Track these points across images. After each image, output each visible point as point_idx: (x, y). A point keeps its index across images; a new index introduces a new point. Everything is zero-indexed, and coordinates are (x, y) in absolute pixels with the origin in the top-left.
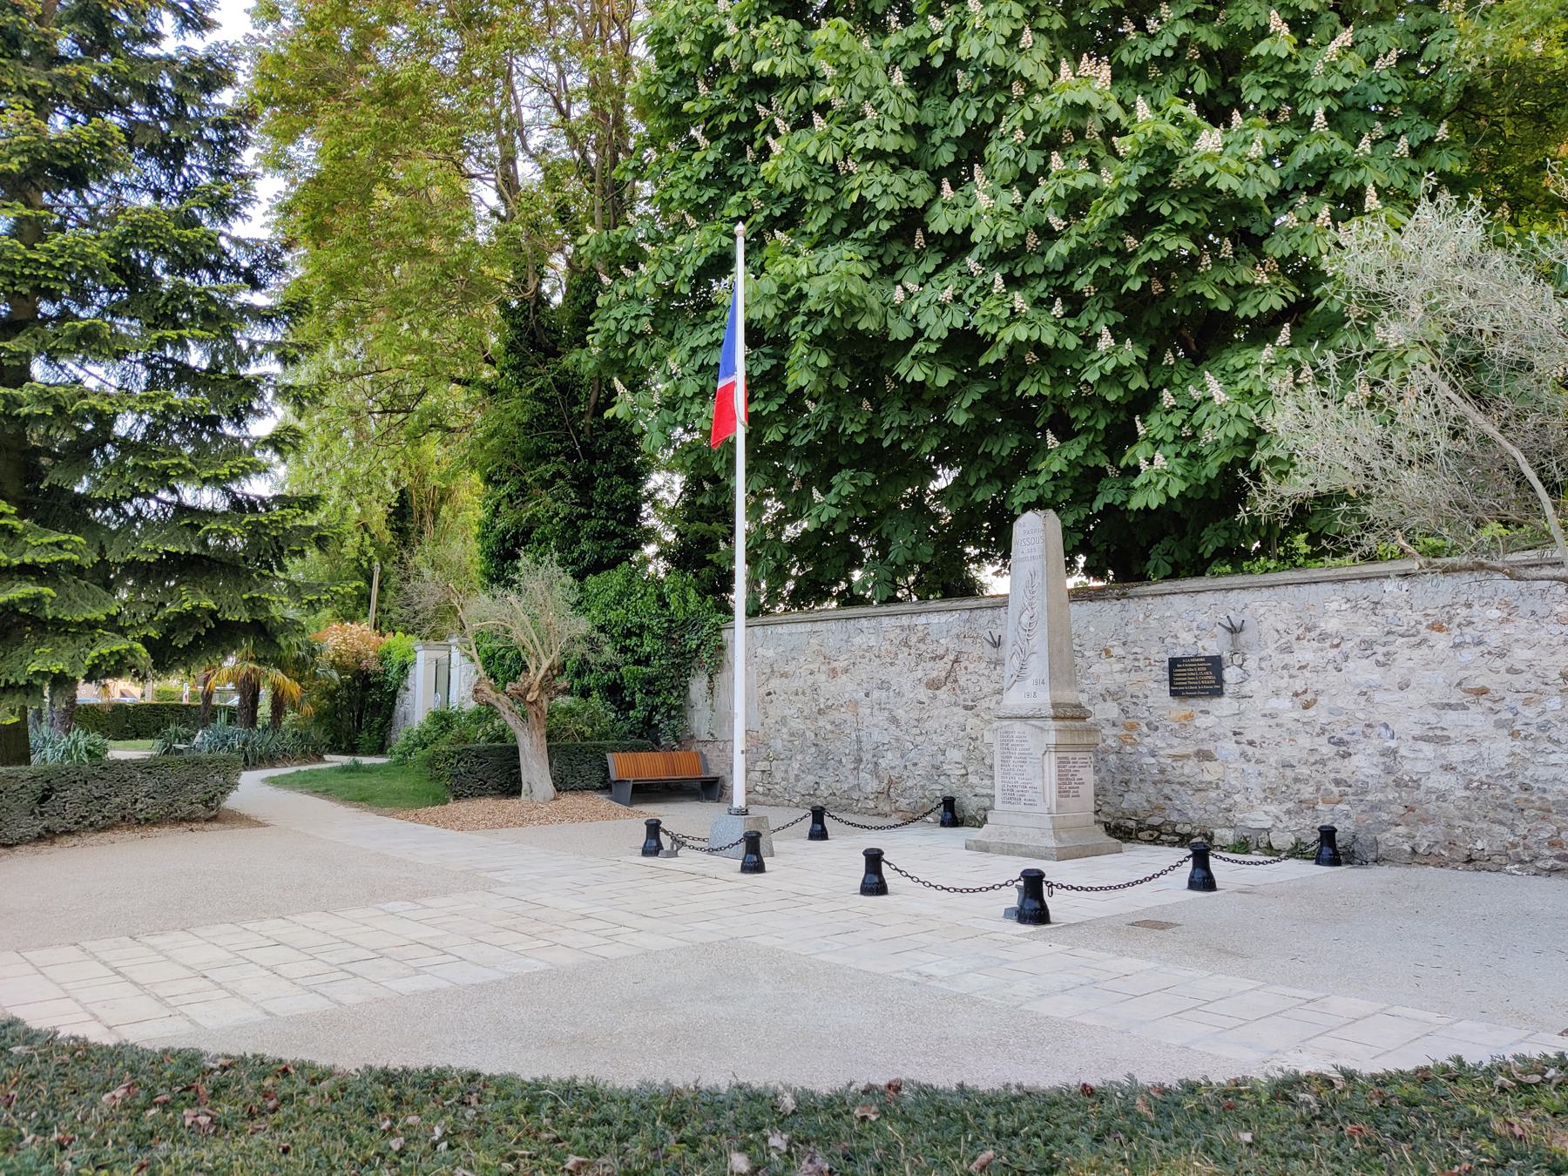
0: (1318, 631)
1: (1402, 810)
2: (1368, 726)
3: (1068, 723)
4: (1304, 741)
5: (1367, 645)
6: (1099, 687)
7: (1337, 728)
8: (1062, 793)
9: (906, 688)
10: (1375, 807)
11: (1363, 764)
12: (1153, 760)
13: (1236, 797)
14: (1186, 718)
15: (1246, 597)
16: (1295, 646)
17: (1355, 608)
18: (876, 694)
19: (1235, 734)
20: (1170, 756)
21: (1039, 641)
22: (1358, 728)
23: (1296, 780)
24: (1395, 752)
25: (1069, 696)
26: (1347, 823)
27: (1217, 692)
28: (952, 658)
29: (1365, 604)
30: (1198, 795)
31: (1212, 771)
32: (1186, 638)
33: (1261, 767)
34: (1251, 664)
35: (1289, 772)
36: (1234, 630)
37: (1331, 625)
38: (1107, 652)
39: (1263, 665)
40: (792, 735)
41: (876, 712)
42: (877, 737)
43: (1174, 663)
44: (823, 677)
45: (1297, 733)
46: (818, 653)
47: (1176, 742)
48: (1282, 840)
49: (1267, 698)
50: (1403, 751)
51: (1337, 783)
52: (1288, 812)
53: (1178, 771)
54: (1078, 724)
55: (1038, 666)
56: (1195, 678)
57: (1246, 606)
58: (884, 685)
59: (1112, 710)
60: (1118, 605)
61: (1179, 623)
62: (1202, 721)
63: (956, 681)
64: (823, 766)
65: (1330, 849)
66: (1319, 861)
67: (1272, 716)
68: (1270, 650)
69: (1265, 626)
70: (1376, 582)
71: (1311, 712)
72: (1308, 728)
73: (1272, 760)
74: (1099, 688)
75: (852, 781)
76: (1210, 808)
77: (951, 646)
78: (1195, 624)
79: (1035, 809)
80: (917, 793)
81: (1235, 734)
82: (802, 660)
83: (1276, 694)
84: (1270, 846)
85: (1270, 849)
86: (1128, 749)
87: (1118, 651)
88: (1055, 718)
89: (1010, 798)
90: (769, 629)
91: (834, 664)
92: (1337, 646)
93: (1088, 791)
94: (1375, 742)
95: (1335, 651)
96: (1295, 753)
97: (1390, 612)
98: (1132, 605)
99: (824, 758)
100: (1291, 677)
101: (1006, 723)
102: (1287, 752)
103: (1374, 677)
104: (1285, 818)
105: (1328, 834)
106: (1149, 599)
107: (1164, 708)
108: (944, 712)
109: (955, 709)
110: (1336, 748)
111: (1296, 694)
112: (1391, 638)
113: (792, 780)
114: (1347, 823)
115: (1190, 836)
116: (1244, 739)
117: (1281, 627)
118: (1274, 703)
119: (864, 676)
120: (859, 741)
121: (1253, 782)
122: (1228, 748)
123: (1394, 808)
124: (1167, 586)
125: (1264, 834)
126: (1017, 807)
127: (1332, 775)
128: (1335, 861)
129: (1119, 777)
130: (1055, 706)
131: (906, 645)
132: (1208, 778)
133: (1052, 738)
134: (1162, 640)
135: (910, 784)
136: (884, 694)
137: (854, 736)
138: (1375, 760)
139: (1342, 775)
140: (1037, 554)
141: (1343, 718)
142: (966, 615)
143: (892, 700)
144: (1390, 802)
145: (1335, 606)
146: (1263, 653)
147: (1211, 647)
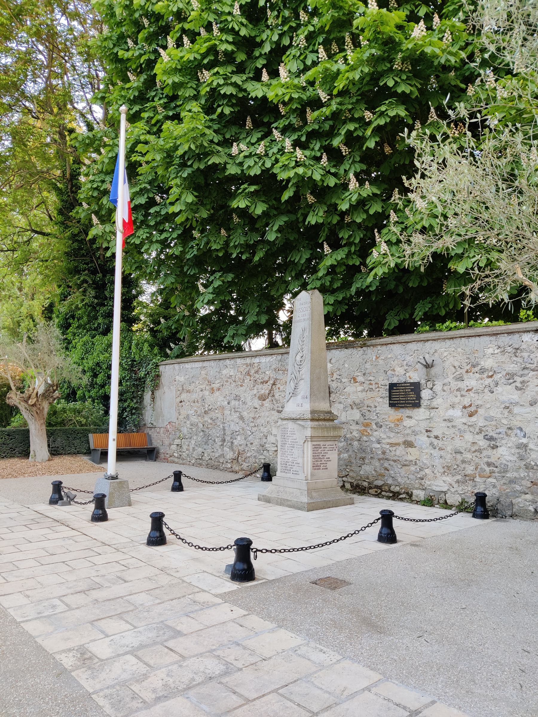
0: (479, 367)
1: (529, 484)
2: (510, 428)
3: (321, 423)
4: (469, 437)
5: (510, 376)
6: (349, 400)
7: (490, 430)
8: (315, 467)
9: (248, 400)
10: (512, 481)
11: (505, 453)
12: (378, 446)
13: (427, 471)
14: (398, 420)
15: (437, 345)
16: (465, 377)
17: (503, 352)
18: (233, 403)
19: (427, 431)
20: (388, 444)
21: (306, 372)
22: (503, 430)
23: (463, 462)
24: (526, 446)
25: (324, 406)
26: (494, 491)
27: (417, 405)
28: (272, 382)
29: (509, 349)
30: (404, 468)
31: (412, 454)
32: (400, 371)
33: (442, 453)
34: (438, 388)
35: (458, 456)
36: (428, 366)
37: (488, 363)
38: (355, 379)
39: (445, 388)
40: (192, 425)
41: (233, 413)
42: (234, 427)
43: (392, 386)
44: (207, 393)
45: (465, 431)
46: (205, 379)
47: (392, 435)
48: (454, 499)
49: (447, 409)
50: (531, 446)
51: (489, 464)
52: (458, 482)
53: (393, 453)
54: (327, 424)
55: (304, 388)
56: (405, 396)
57: (436, 351)
58: (237, 398)
59: (356, 415)
60: (361, 351)
61: (396, 362)
62: (407, 423)
63: (273, 396)
64: (206, 443)
65: (481, 508)
66: (475, 516)
67: (450, 421)
68: (450, 379)
69: (447, 364)
70: (517, 336)
71: (474, 419)
72: (471, 429)
73: (449, 449)
74: (350, 401)
75: (220, 452)
76: (411, 476)
77: (272, 375)
78: (405, 363)
79: (297, 477)
80: (252, 460)
81: (427, 431)
82: (197, 383)
83: (453, 406)
84: (446, 502)
85: (446, 505)
86: (365, 438)
87: (360, 379)
88: (312, 420)
89: (285, 471)
90: (182, 365)
91: (213, 385)
92: (491, 376)
93: (333, 466)
94: (513, 439)
95: (490, 380)
96: (463, 444)
97: (525, 355)
98: (369, 350)
99: (207, 439)
100: (462, 396)
101: (285, 422)
102: (458, 443)
103: (513, 397)
104: (455, 485)
105: (481, 498)
106: (379, 347)
107: (386, 414)
108: (267, 414)
109: (273, 412)
110: (488, 442)
111: (465, 407)
112: (526, 372)
113: (191, 450)
114: (494, 491)
115: (399, 493)
116: (432, 435)
117: (457, 364)
118: (451, 413)
119: (227, 393)
120: (224, 430)
121: (437, 462)
122: (422, 440)
123: (524, 482)
124: (390, 339)
125: (442, 495)
126: (288, 475)
127: (486, 460)
128: (485, 515)
129: (359, 455)
130: (313, 412)
131: (248, 374)
132: (410, 458)
133: (309, 433)
134: (386, 372)
135: (248, 455)
136: (237, 403)
137: (221, 426)
138: (513, 451)
139: (492, 460)
140: (307, 317)
141: (494, 423)
142: (279, 357)
143: (241, 406)
144: (522, 479)
145: (490, 351)
146: (446, 381)
147: (414, 377)
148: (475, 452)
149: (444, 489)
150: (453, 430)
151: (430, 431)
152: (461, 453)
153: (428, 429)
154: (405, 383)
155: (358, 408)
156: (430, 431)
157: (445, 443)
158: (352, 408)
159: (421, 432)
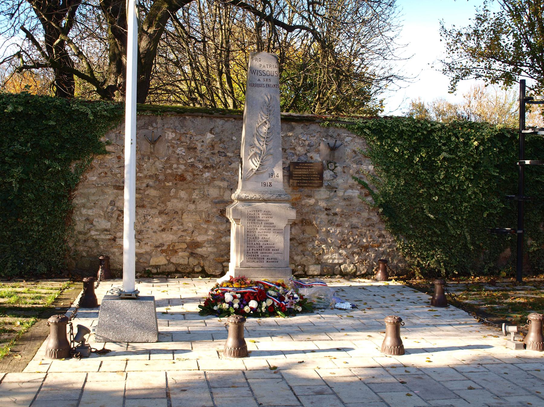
14: (296, 199)
32: (300, 150)
34: (339, 169)
78: (307, 143)
81: (326, 209)
118: (350, 192)
148: (369, 226)
151: (329, 209)
154: (306, 162)
156: (329, 209)
159: (320, 210)
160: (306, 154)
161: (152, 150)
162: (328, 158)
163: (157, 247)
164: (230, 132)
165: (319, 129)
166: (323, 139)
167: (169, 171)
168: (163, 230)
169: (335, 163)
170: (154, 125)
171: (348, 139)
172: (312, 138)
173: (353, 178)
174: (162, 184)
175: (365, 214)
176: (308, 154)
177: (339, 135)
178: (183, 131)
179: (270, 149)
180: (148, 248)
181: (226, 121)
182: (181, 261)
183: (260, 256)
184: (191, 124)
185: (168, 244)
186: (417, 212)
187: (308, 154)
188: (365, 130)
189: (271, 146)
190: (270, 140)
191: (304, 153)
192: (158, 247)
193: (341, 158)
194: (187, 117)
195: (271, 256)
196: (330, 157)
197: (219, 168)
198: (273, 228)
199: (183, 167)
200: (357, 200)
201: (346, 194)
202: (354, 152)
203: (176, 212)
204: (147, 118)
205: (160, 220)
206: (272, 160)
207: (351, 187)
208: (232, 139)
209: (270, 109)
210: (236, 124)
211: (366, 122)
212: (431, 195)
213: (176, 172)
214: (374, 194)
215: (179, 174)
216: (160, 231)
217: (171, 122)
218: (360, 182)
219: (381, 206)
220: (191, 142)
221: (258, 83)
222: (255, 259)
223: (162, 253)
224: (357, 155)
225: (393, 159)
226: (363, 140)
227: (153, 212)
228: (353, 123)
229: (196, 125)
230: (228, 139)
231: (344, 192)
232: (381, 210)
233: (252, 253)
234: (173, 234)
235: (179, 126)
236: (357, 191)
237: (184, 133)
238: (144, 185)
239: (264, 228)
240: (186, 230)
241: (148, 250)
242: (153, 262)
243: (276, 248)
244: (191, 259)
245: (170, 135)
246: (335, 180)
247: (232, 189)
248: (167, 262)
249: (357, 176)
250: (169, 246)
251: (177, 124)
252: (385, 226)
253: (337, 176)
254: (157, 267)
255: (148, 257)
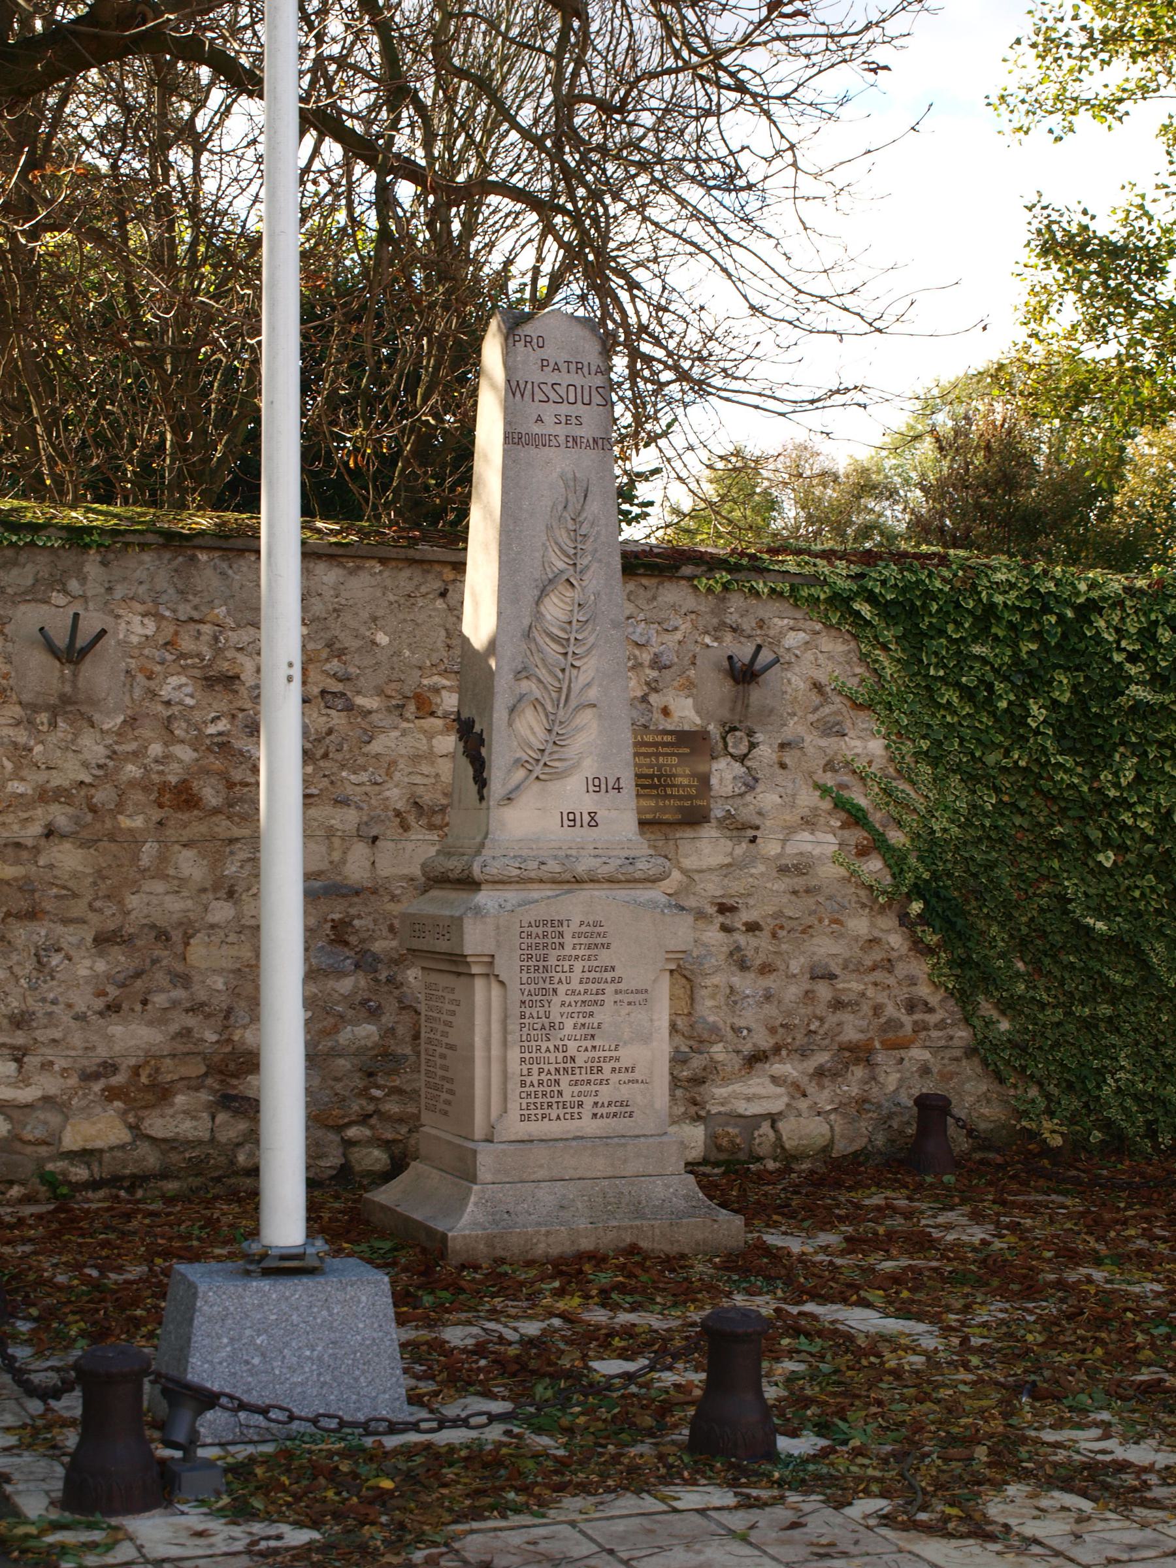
33: (769, 982)
34: (766, 752)
35: (824, 991)
49: (790, 830)
52: (819, 1073)
73: (795, 968)
81: (723, 909)
104: (811, 1089)
118: (805, 842)
125: (766, 1127)
148: (873, 969)
149: (776, 1106)
150: (810, 901)
152: (832, 977)
153: (730, 902)
155: (431, 827)
157: (784, 947)
158: (405, 827)
160: (644, 699)
161: (68, 689)
162: (725, 713)
163: (88, 1077)
164: (365, 615)
165: (690, 602)
166: (708, 640)
167: (132, 770)
168: (113, 1008)
169: (750, 733)
170: (74, 585)
171: (793, 639)
172: (666, 637)
173: (817, 786)
174: (108, 824)
175: (859, 925)
176: (654, 698)
177: (761, 623)
178: (184, 611)
179: (588, 685)
180: (48, 1084)
181: (352, 572)
182: (187, 1128)
183: (567, 1097)
184: (216, 582)
185: (133, 1062)
186: (1042, 910)
187: (654, 698)
188: (856, 606)
189: (591, 674)
190: (589, 651)
191: (639, 694)
192: (96, 1076)
193: (771, 711)
194: (203, 557)
195: (606, 1093)
196: (732, 710)
197: (325, 756)
198: (613, 987)
199: (185, 753)
200: (830, 872)
201: (791, 849)
202: (817, 687)
203: (162, 936)
204: (43, 559)
205: (101, 966)
206: (594, 725)
207: (808, 823)
208: (374, 643)
209: (583, 531)
210: (388, 582)
211: (862, 576)
212: (1090, 846)
213: (161, 773)
214: (890, 848)
215: (173, 779)
216: (101, 1014)
217: (140, 574)
218: (841, 804)
219: (917, 891)
220: (218, 652)
221: (537, 429)
222: (550, 1106)
223: (110, 1100)
224: (826, 700)
225: (955, 713)
226: (846, 642)
227: (69, 936)
228: (816, 580)
229: (236, 586)
230: (357, 643)
231: (784, 841)
232: (916, 907)
233: (540, 1083)
234: (150, 1023)
235: (171, 591)
236: (830, 838)
237: (192, 620)
238: (36, 829)
239: (582, 988)
240: (203, 1004)
241: (52, 1091)
242: (71, 1140)
243: (624, 1063)
244: (221, 1117)
245: (136, 627)
246: (749, 798)
247: (375, 839)
248: (125, 1136)
249: (829, 780)
250: (136, 1071)
251: (162, 581)
252: (927, 968)
253: (756, 780)
254: (85, 1155)
255: (54, 1119)
